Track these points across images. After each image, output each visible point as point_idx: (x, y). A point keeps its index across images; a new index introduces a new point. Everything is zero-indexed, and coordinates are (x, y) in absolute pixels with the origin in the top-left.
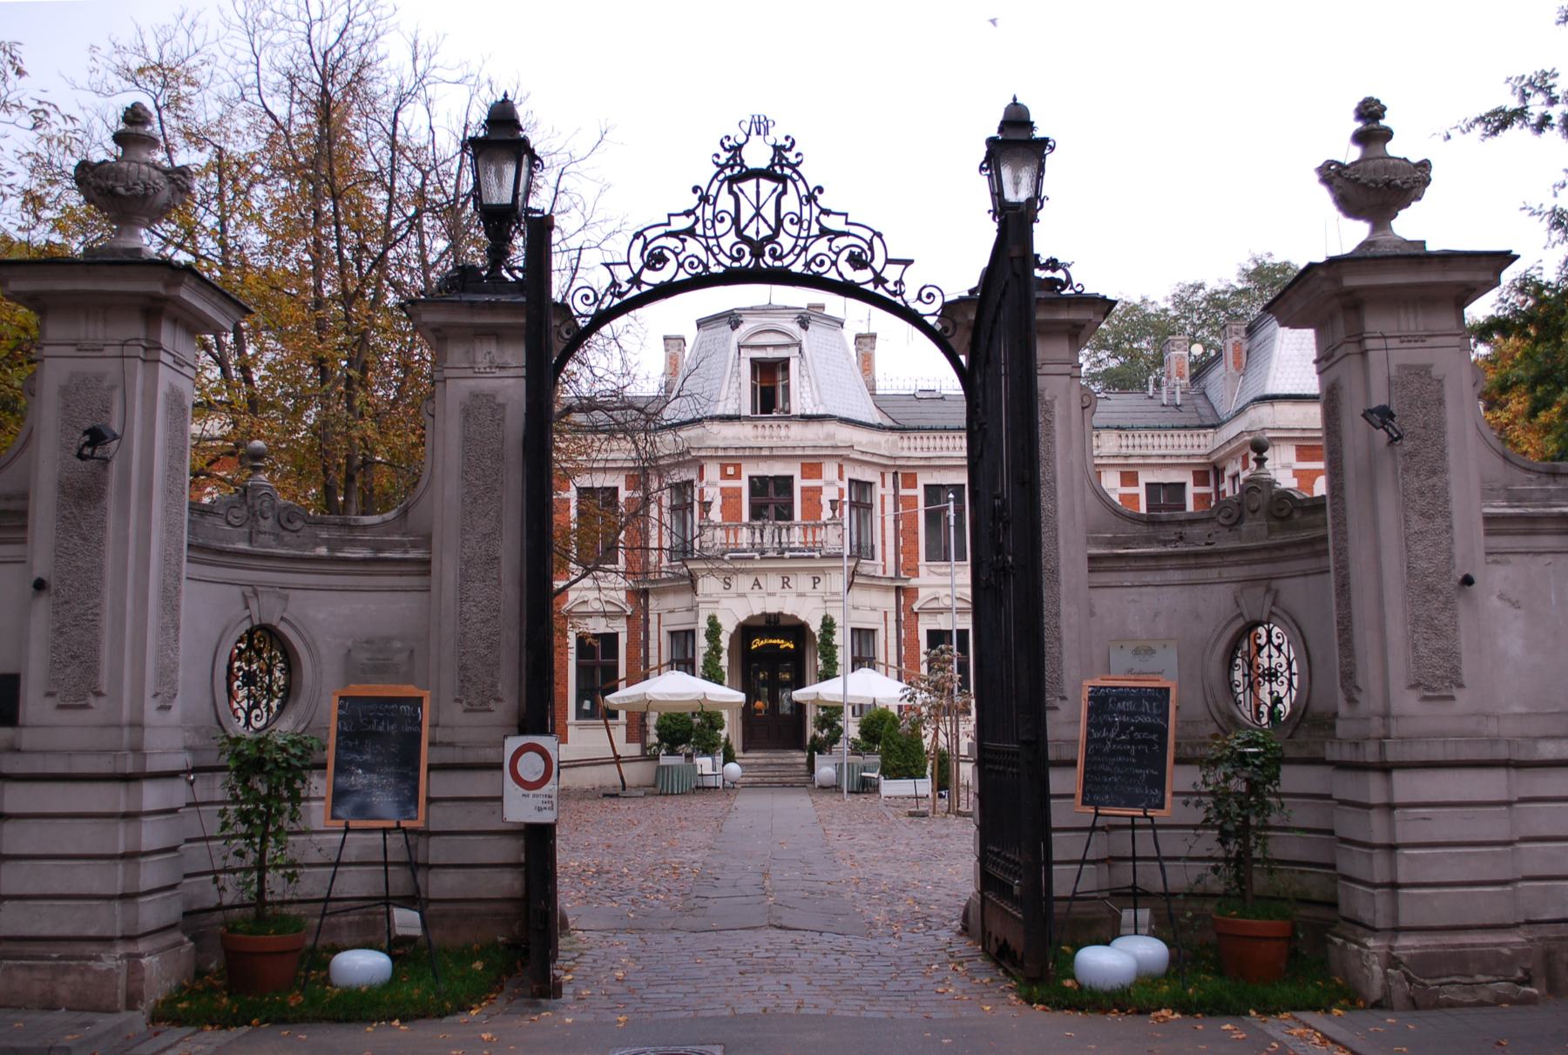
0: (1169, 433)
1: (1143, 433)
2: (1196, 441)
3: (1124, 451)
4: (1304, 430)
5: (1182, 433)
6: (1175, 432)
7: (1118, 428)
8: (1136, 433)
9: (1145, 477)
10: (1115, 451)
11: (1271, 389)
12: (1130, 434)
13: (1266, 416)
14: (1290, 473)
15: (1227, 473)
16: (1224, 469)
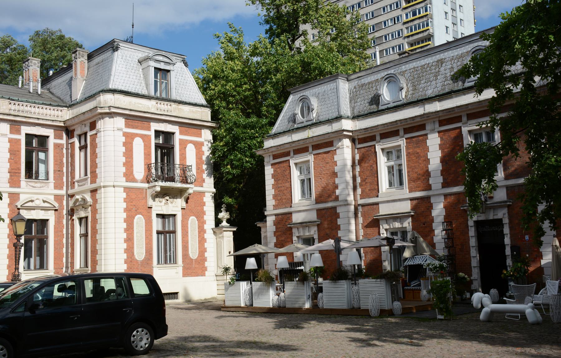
0: (41, 106)
1: (25, 104)
2: (56, 113)
3: (12, 113)
4: (131, 110)
5: (48, 107)
6: (45, 107)
7: (9, 99)
8: (21, 103)
9: (25, 130)
10: (7, 112)
11: (111, 86)
12: (17, 103)
13: (107, 99)
14: (121, 133)
15: (76, 133)
16: (74, 130)
